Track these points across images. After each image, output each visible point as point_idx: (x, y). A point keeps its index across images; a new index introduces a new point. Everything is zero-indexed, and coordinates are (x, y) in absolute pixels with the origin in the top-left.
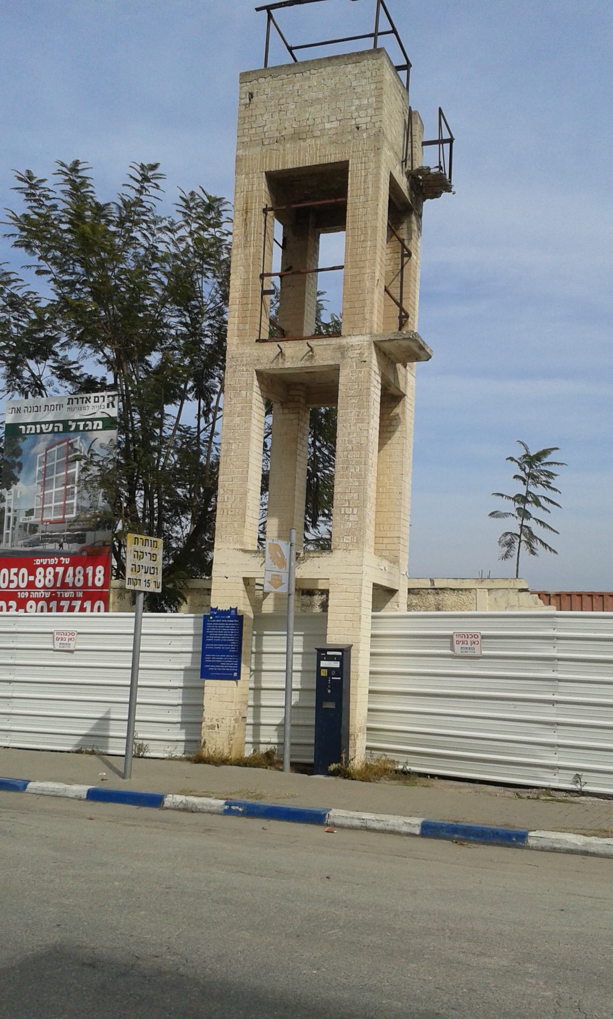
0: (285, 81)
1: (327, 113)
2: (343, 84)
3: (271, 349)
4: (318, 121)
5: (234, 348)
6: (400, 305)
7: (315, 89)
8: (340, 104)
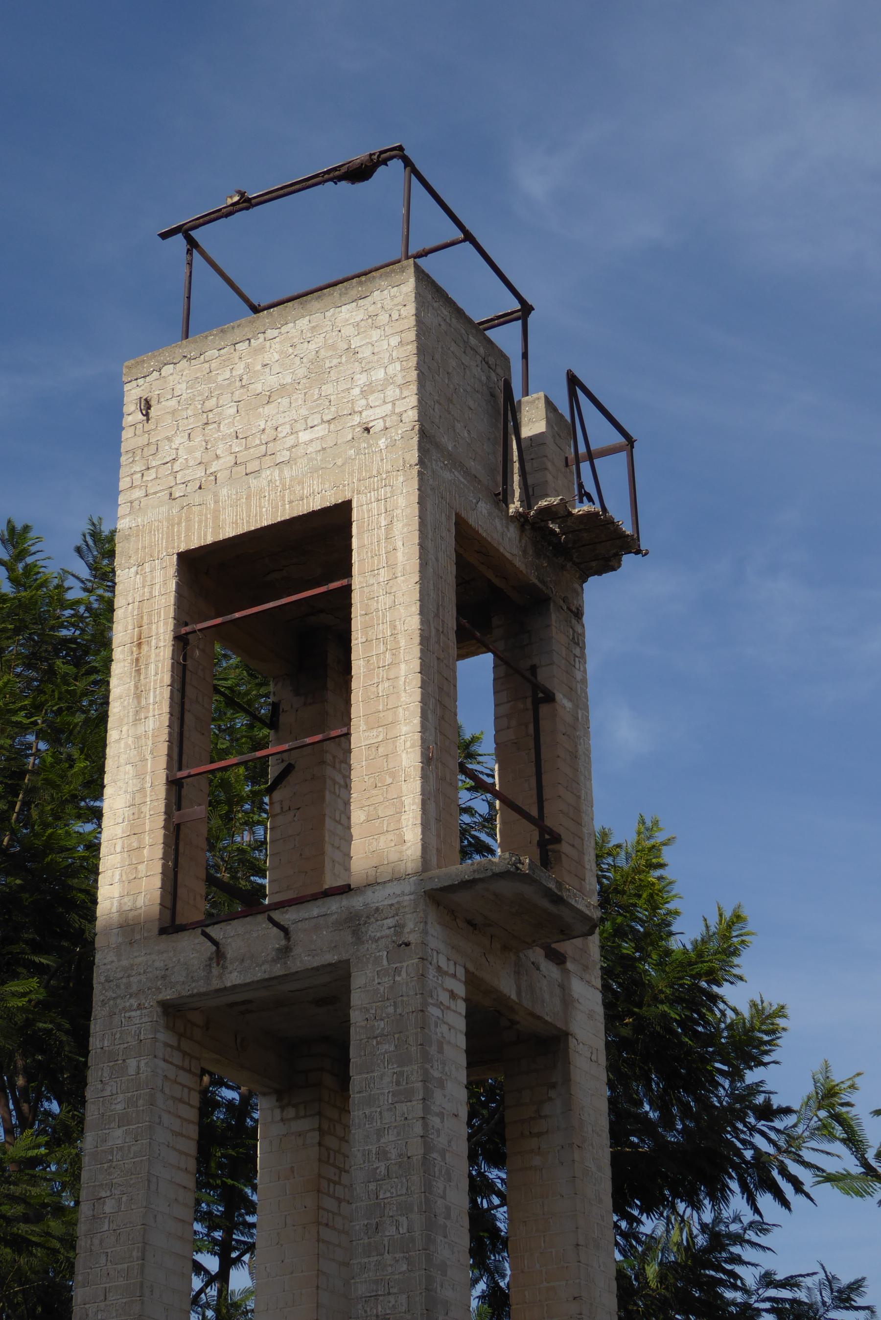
0: (214, 365)
1: (304, 412)
2: (333, 347)
3: (191, 949)
4: (284, 430)
5: (111, 957)
6: (538, 822)
7: (276, 368)
8: (327, 389)
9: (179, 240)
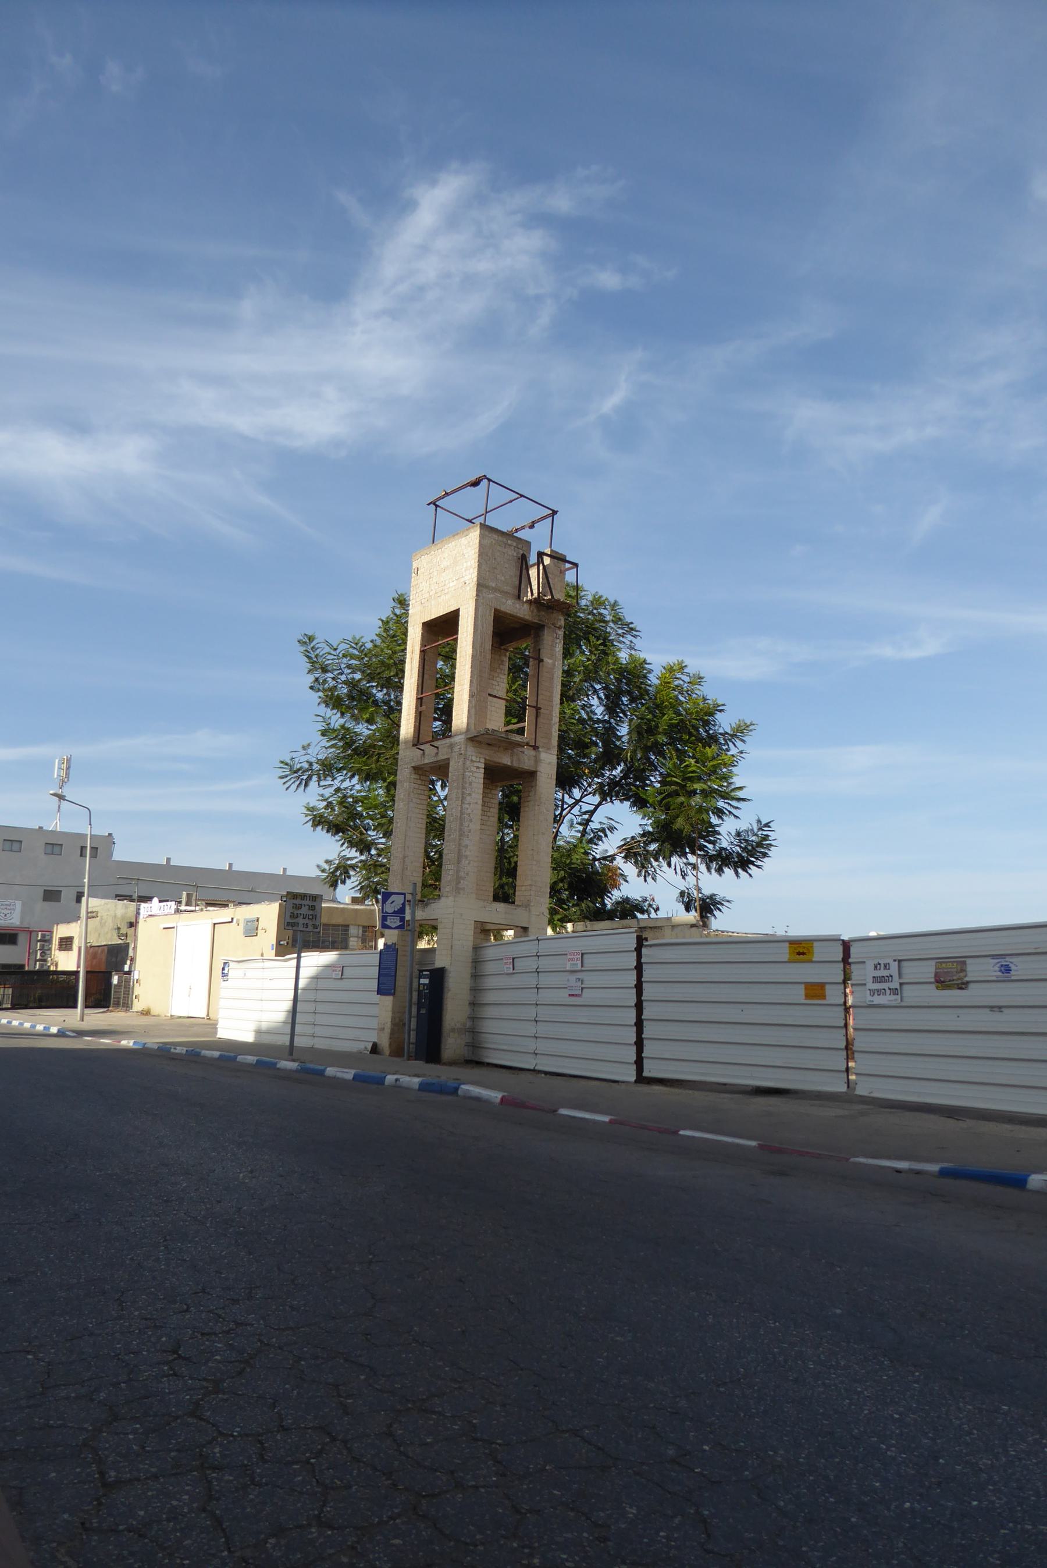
9: (433, 507)
